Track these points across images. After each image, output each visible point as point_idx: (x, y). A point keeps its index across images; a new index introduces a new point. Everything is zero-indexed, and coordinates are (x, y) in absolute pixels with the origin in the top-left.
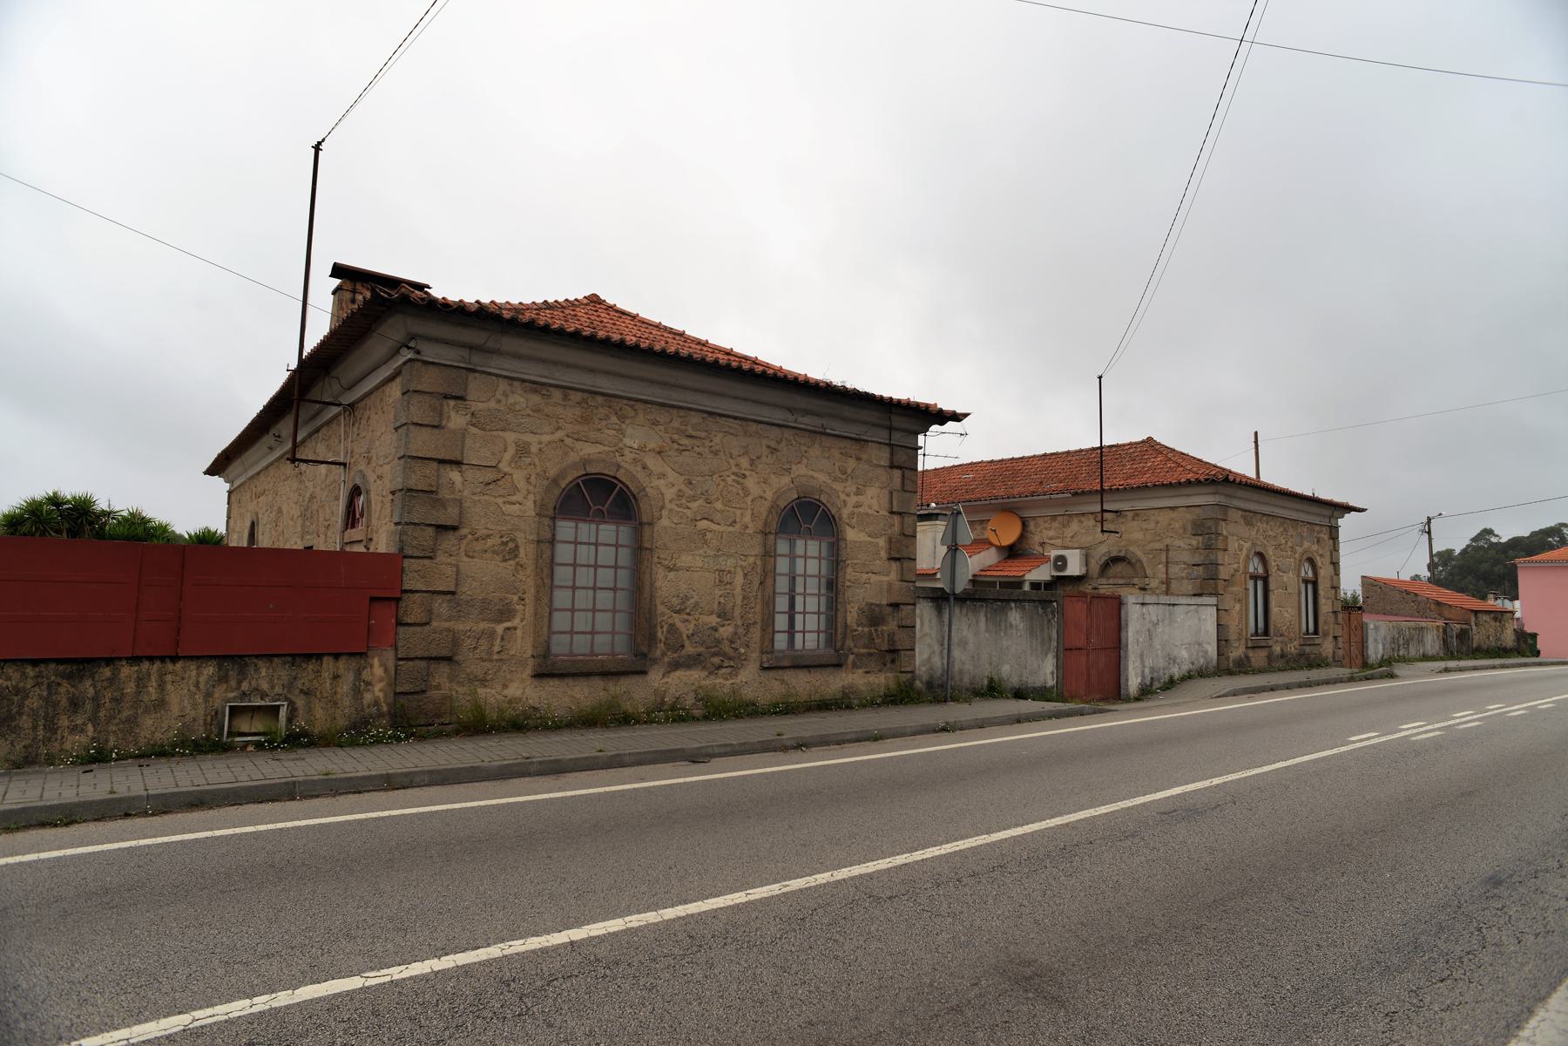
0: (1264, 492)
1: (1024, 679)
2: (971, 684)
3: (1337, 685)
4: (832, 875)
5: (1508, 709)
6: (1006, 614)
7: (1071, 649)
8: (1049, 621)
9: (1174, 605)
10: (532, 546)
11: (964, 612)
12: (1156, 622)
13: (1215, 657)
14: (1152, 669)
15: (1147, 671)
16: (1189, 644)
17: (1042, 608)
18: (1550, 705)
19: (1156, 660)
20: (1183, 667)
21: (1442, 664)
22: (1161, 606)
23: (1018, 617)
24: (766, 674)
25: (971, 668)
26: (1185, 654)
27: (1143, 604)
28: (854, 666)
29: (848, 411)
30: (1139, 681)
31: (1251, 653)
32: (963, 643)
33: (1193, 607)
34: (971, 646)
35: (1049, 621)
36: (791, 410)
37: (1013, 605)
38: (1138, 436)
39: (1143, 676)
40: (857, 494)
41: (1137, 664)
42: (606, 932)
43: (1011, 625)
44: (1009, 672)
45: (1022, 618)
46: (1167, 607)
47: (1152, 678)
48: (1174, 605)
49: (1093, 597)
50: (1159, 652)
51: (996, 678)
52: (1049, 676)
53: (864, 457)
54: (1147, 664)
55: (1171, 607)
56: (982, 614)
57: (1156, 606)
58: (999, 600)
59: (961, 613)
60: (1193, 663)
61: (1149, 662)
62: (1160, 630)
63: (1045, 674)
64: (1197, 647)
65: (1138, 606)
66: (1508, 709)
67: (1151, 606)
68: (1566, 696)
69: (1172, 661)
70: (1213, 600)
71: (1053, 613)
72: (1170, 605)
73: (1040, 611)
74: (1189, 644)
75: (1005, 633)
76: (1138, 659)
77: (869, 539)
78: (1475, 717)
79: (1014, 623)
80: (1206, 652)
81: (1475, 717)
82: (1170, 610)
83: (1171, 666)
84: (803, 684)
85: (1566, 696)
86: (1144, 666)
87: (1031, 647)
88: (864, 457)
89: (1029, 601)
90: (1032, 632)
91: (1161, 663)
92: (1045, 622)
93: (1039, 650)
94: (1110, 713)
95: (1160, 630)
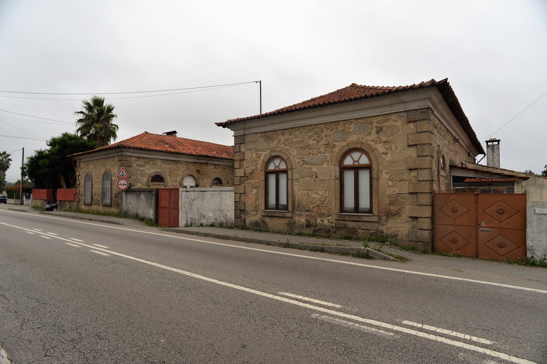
0: (254, 120)
1: (145, 215)
2: (132, 214)
3: (251, 244)
4: (471, 348)
5: (42, 233)
6: (140, 196)
7: (163, 208)
8: (152, 198)
9: (204, 191)
10: (338, 180)
11: (130, 194)
12: (194, 199)
13: (234, 218)
14: (191, 219)
15: (189, 219)
16: (214, 210)
17: (150, 194)
18: (105, 254)
19: (194, 215)
20: (209, 220)
21: (283, 239)
22: (197, 192)
23: (143, 196)
24: (103, 207)
25: (132, 210)
26: (211, 214)
27: (187, 191)
28: (114, 207)
29: (386, 101)
30: (185, 222)
31: (267, 220)
32: (130, 203)
33: (216, 192)
34: (132, 204)
35: (152, 198)
36: (105, 155)
37: (142, 193)
38: (348, 84)
39: (187, 221)
40: (114, 169)
41: (184, 216)
42: (483, 352)
43: (142, 199)
44: (141, 212)
45: (144, 197)
46: (200, 193)
47: (191, 223)
48: (204, 191)
49: (171, 189)
50: (196, 212)
51: (137, 213)
52: (152, 215)
53: (115, 160)
54: (189, 216)
55: (203, 192)
56: (135, 195)
57: (194, 192)
58: (138, 191)
59: (151, 195)
60: (216, 220)
61: (190, 216)
62: (196, 202)
63: (150, 215)
64: (219, 212)
65: (185, 192)
66: (42, 233)
67: (191, 193)
68: (1, 223)
69: (202, 217)
70: (232, 188)
71: (153, 195)
72: (201, 191)
73: (149, 194)
74: (214, 210)
75: (140, 201)
76: (185, 214)
77: (116, 179)
78: (106, 251)
79: (142, 198)
80: (226, 215)
81: (106, 251)
82: (202, 194)
83: (202, 219)
84: (107, 209)
85: (1, 223)
86: (187, 217)
87: (147, 205)
88: (115, 160)
89: (146, 191)
90: (147, 202)
91: (196, 217)
92: (151, 198)
93: (149, 207)
94: (121, 225)
95: (196, 202)
